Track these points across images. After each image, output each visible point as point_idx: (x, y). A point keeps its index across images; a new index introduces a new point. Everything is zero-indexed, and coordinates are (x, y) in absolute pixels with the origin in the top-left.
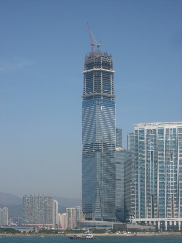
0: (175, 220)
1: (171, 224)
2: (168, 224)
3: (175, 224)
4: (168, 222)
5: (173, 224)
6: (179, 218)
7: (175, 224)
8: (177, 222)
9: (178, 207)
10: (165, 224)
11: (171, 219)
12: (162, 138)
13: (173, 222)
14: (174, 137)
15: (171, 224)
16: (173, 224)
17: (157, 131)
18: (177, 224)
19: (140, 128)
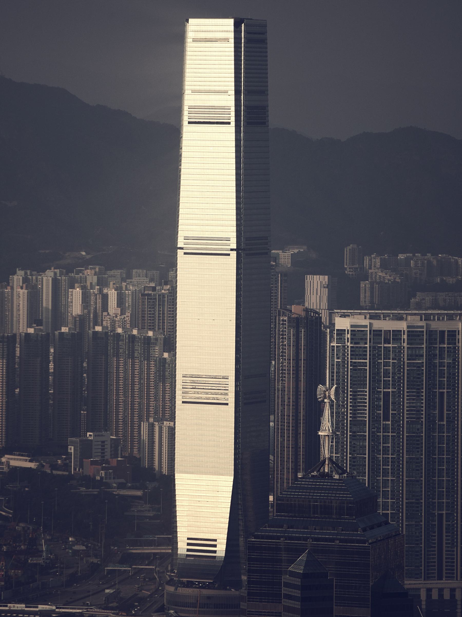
0: (446, 584)
1: (435, 596)
2: (429, 596)
3: (447, 596)
4: (429, 590)
5: (441, 595)
6: (457, 579)
7: (447, 596)
8: (453, 590)
9: (455, 549)
10: (419, 596)
11: (435, 584)
12: (417, 356)
13: (441, 590)
14: (449, 356)
15: (435, 596)
16: (441, 595)
17: (406, 337)
18: (453, 596)
19: (352, 326)
